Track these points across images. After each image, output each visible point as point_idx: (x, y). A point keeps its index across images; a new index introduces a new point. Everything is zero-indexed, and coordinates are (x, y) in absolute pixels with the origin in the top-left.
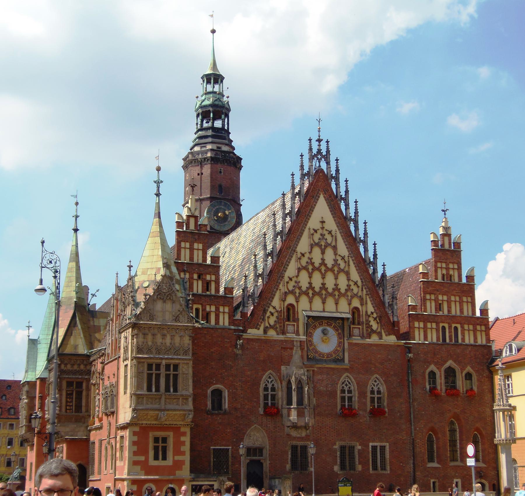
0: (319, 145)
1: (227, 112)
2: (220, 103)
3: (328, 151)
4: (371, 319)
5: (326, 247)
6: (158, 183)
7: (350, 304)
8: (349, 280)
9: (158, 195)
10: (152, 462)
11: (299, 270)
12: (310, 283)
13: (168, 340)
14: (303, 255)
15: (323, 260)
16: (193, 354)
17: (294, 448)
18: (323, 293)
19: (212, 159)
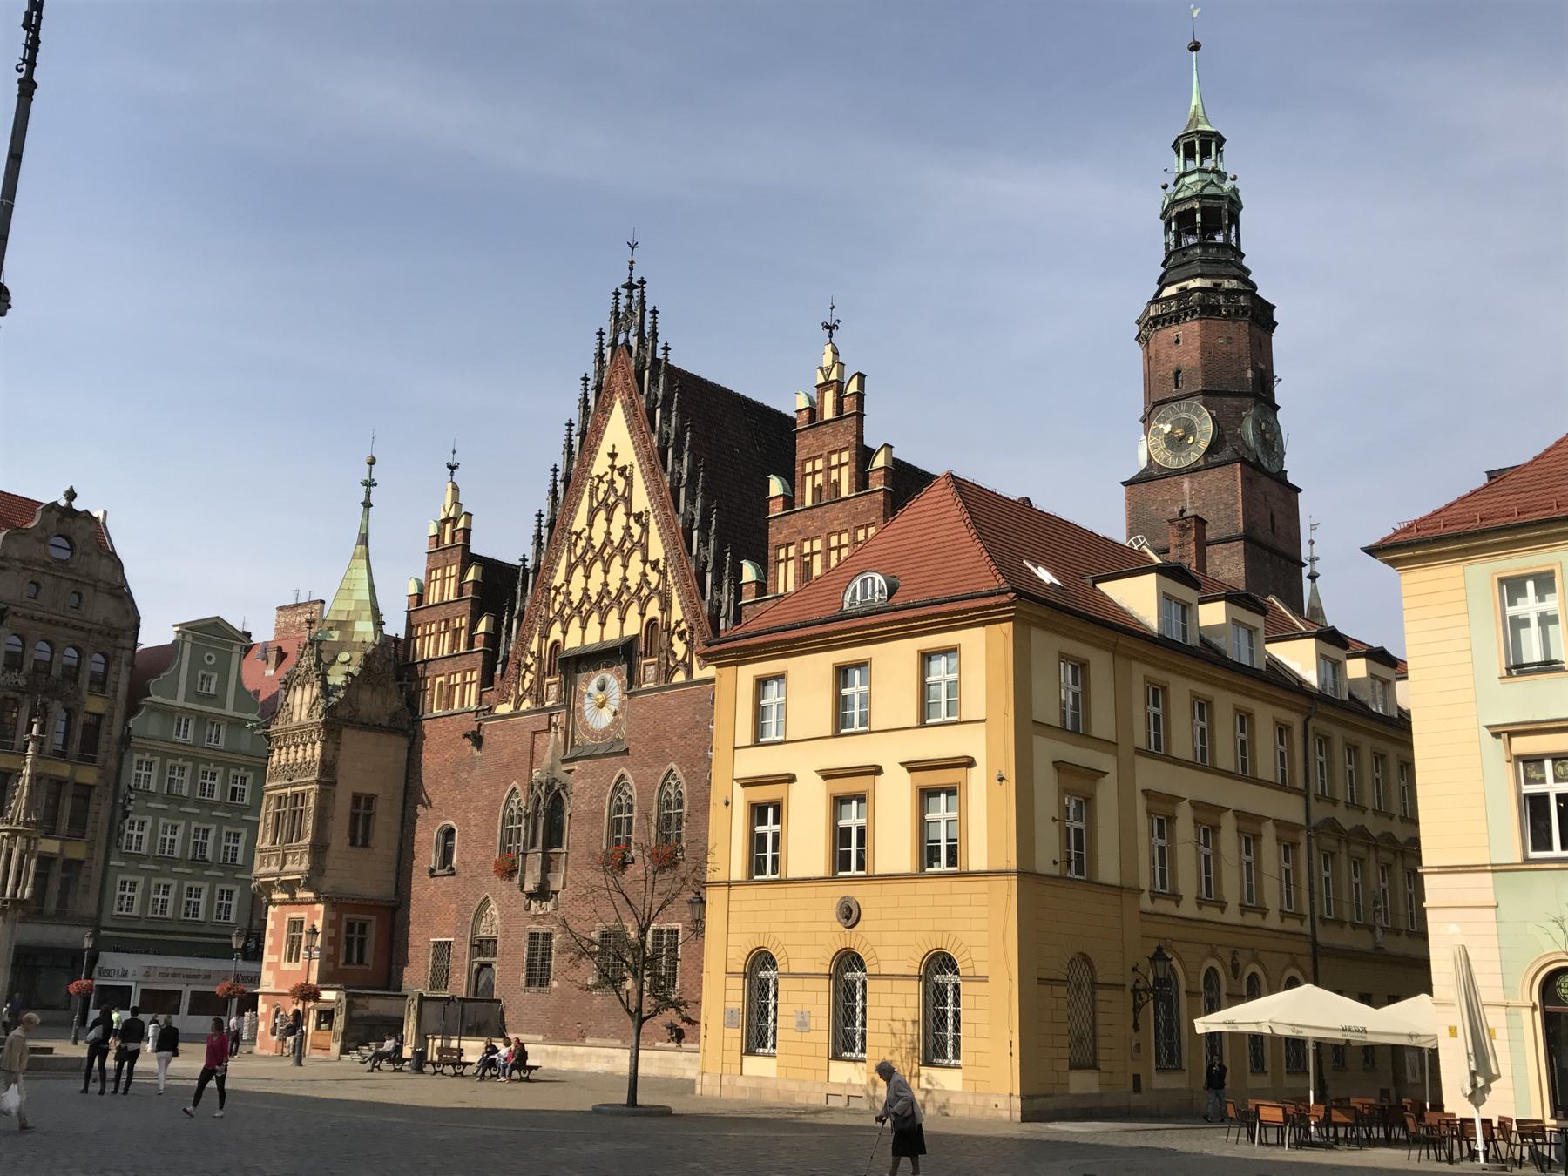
0: (630, 297)
1: (1209, 203)
2: (1188, 193)
3: (643, 302)
4: (675, 639)
5: (615, 505)
6: (369, 484)
7: (642, 615)
8: (645, 561)
9: (367, 505)
10: (286, 966)
11: (571, 569)
12: (586, 589)
13: (300, 753)
14: (579, 535)
15: (608, 533)
16: (321, 773)
17: (533, 936)
18: (601, 606)
19: (1156, 320)
